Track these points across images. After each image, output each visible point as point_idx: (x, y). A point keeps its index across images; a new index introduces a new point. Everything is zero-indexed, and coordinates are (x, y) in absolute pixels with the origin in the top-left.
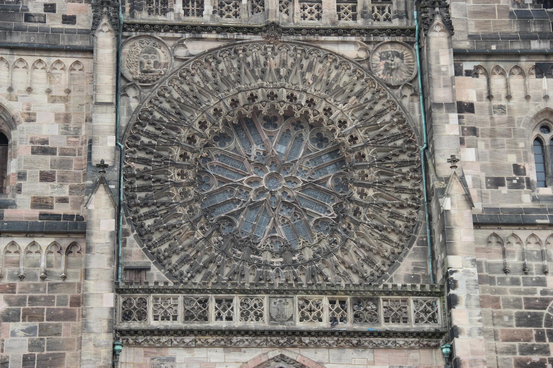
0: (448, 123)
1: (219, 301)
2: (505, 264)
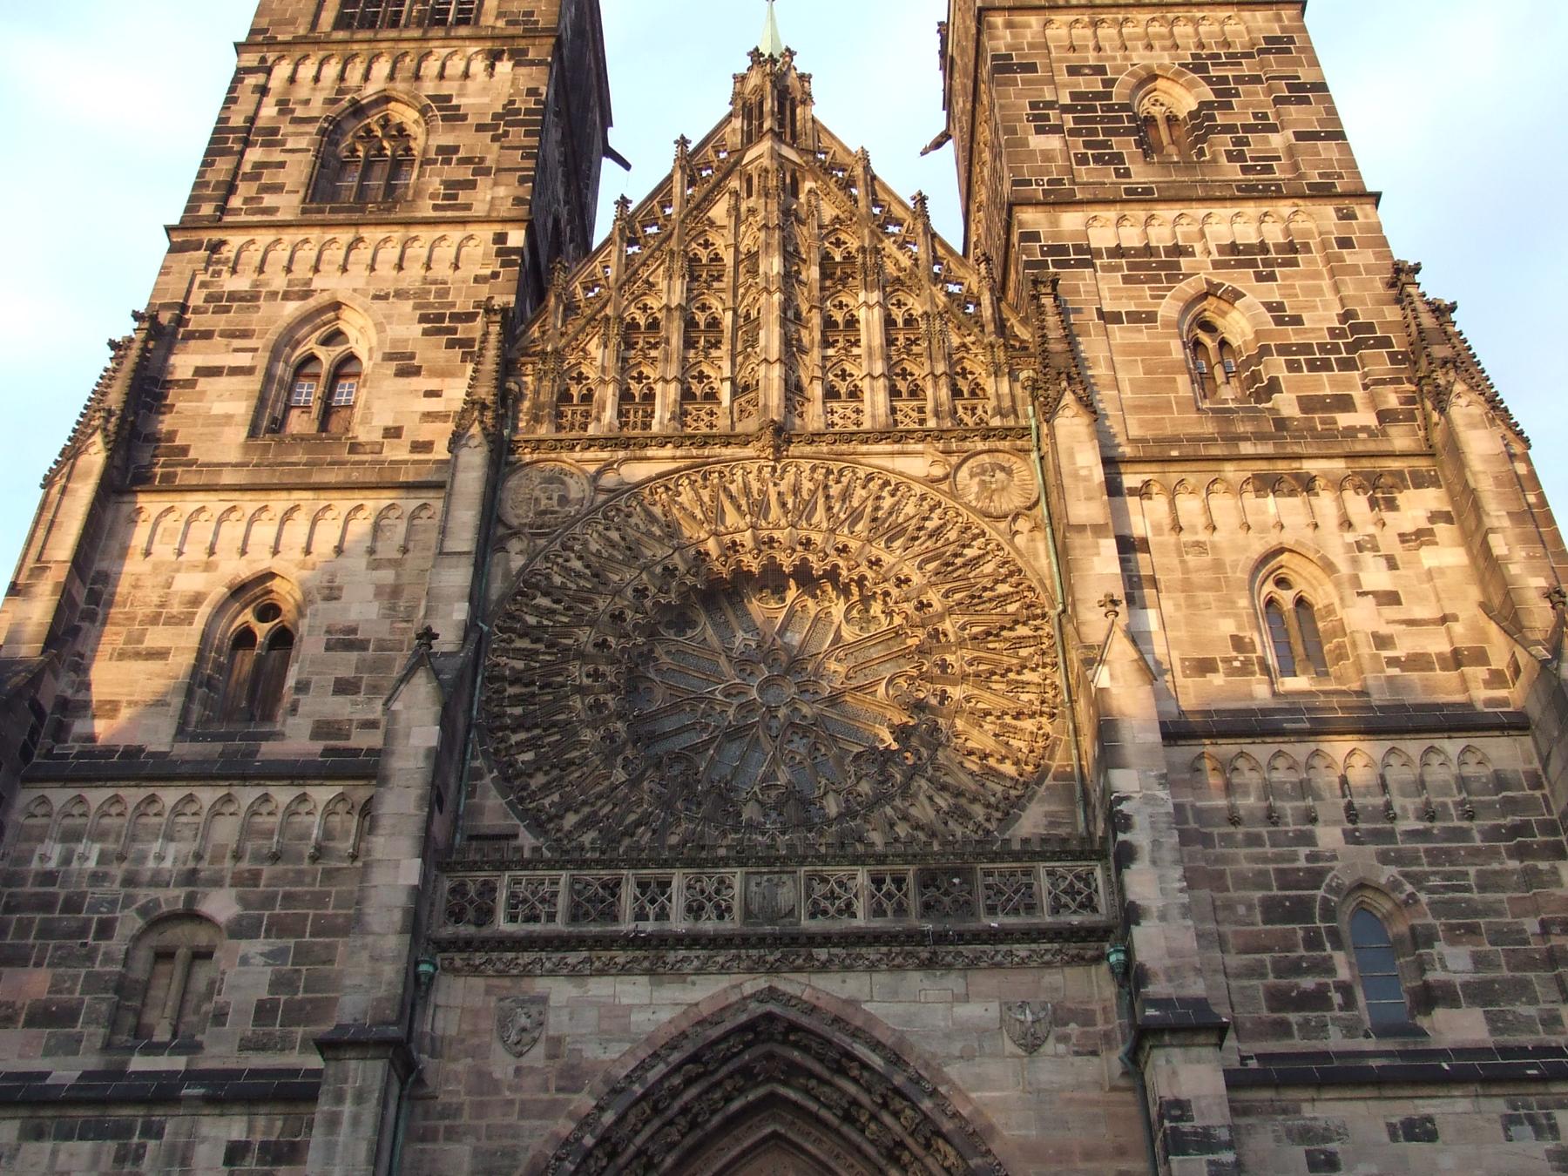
0: (1098, 554)
1: (643, 886)
2: (1232, 808)
